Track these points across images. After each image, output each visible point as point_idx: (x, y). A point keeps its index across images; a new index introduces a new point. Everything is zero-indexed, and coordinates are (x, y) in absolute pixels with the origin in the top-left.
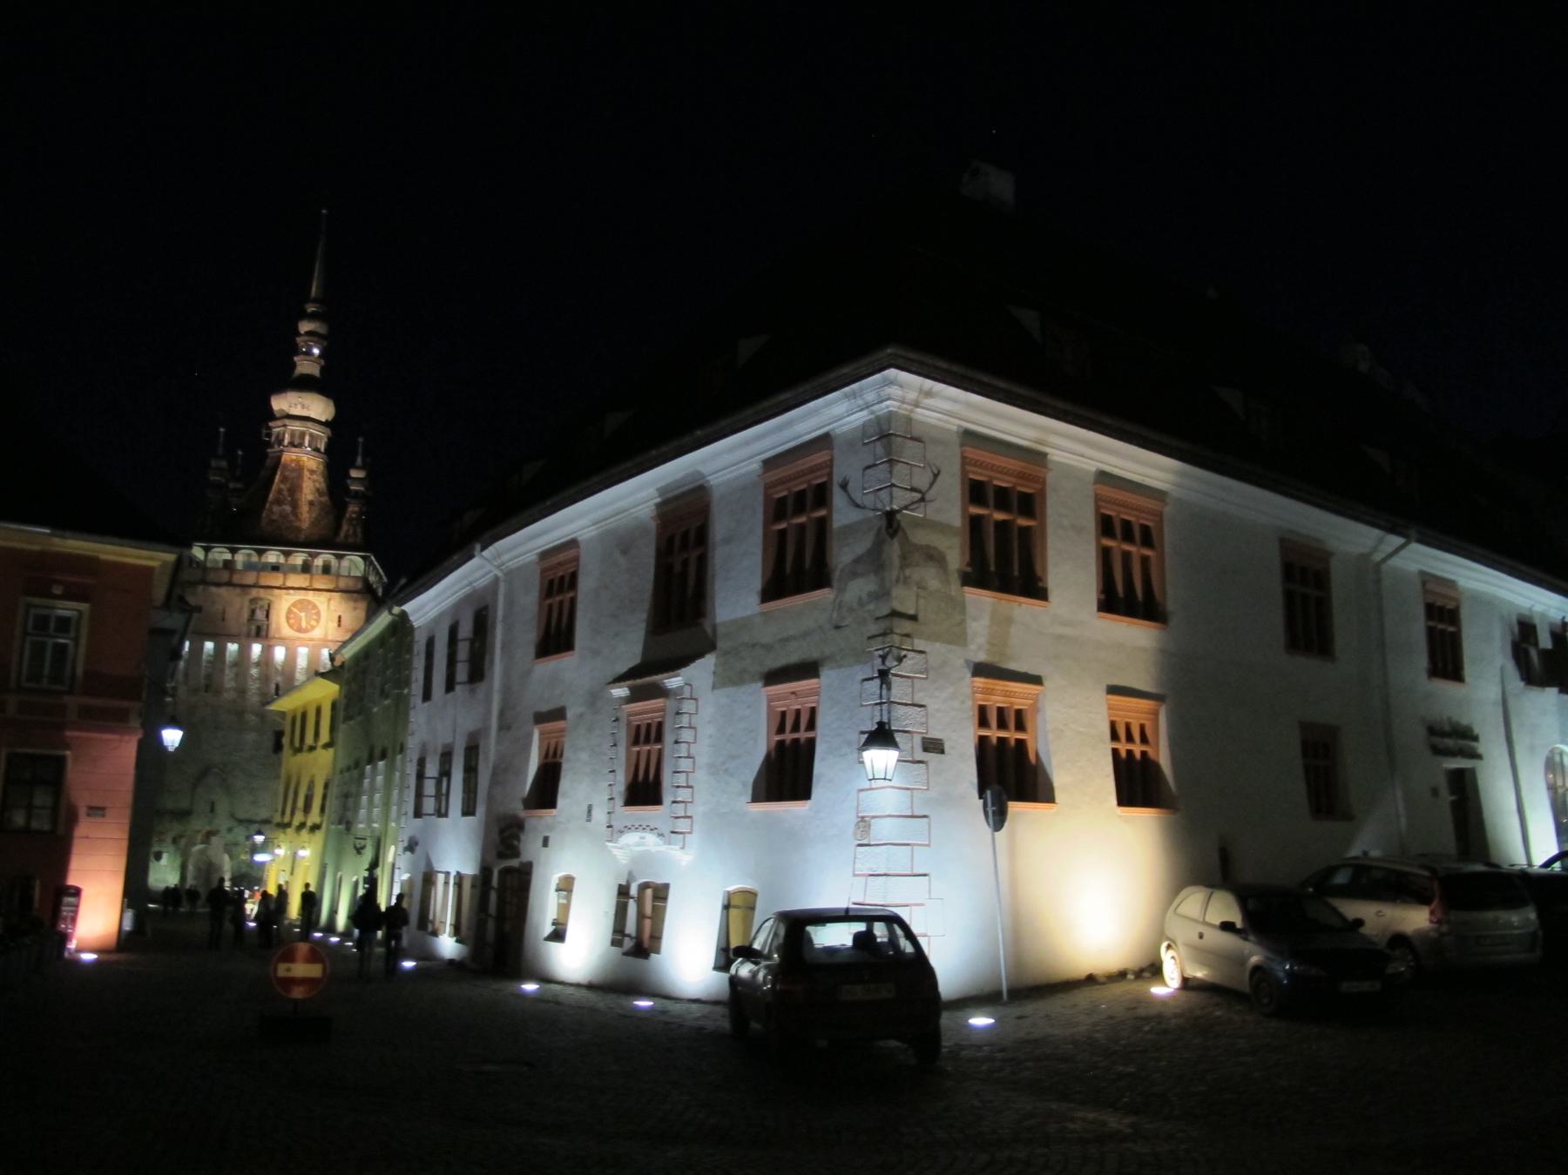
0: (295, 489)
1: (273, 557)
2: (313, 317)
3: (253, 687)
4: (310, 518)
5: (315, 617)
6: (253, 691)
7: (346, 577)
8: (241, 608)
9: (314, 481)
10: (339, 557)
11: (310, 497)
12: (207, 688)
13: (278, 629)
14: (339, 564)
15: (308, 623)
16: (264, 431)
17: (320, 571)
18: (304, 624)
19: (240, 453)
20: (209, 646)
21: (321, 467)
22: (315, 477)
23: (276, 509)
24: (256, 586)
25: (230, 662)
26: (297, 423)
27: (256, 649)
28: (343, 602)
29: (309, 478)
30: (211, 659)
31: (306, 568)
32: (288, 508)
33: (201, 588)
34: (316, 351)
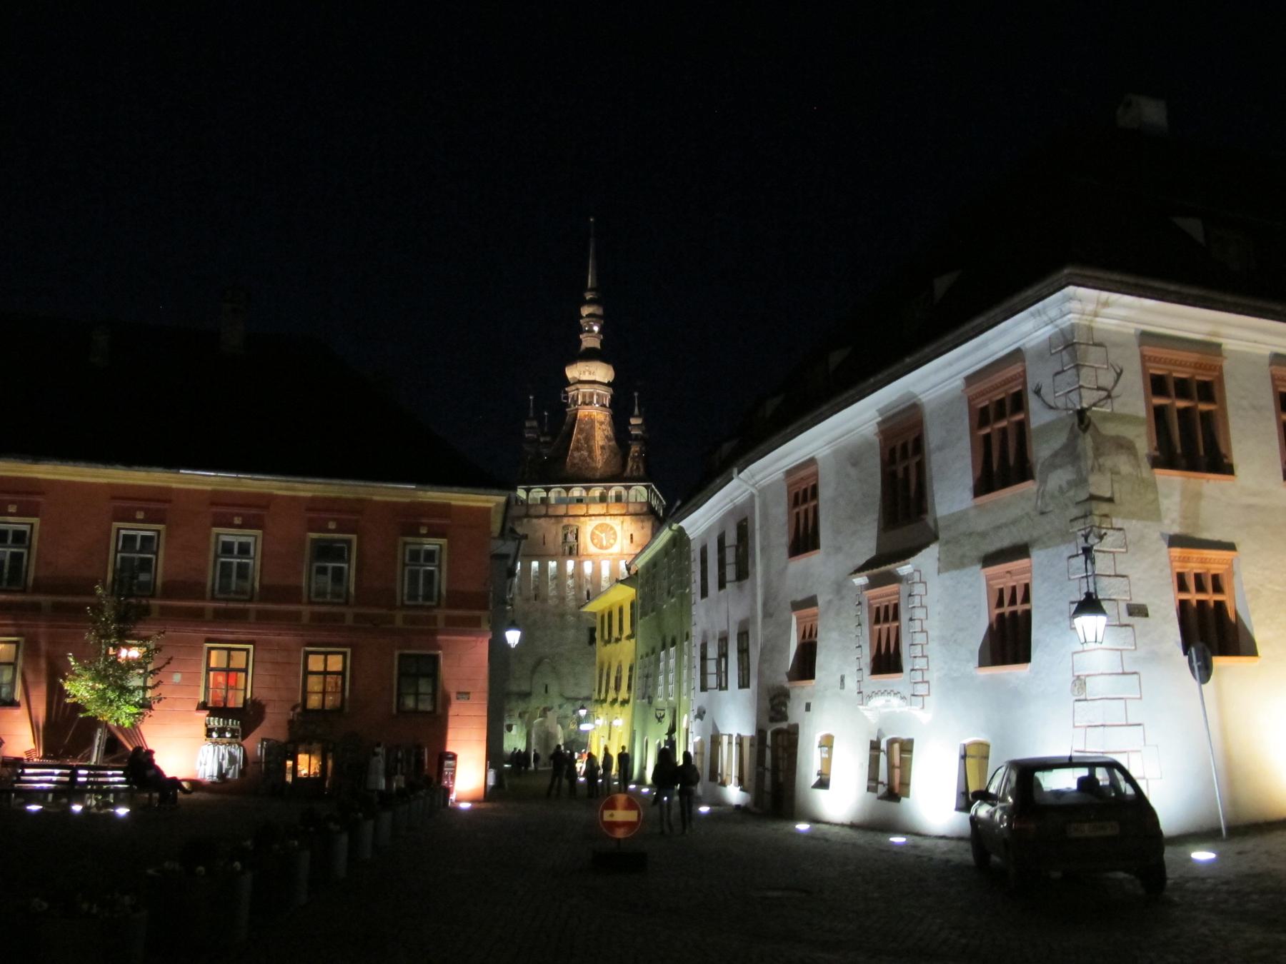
0: (589, 438)
1: (577, 492)
2: (591, 302)
3: (570, 594)
4: (603, 459)
6: (570, 598)
7: (634, 503)
8: (557, 534)
9: (603, 430)
10: (628, 488)
11: (601, 443)
12: (536, 597)
13: (586, 547)
14: (628, 493)
15: (608, 541)
16: (563, 395)
17: (614, 499)
18: (604, 543)
19: (546, 414)
20: (535, 564)
21: (608, 418)
22: (604, 427)
23: (576, 454)
24: (566, 515)
25: (551, 576)
26: (587, 386)
27: (570, 565)
30: (537, 574)
31: (603, 499)
32: (586, 453)
33: (525, 520)
34: (596, 329)
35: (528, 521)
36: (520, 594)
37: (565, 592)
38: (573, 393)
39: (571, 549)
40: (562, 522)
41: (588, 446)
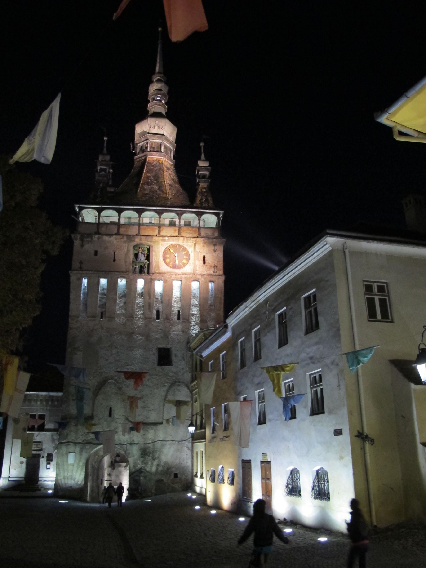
0: (158, 176)
3: (139, 313)
5: (185, 257)
8: (128, 251)
13: (158, 266)
15: (180, 261)
18: (177, 262)
20: (103, 282)
21: (172, 167)
23: (146, 187)
27: (140, 283)
28: (205, 246)
29: (167, 171)
30: (106, 292)
31: (172, 224)
32: (156, 187)
35: (99, 238)
37: (133, 309)
38: (141, 144)
39: (141, 268)
40: (134, 241)
41: (158, 182)
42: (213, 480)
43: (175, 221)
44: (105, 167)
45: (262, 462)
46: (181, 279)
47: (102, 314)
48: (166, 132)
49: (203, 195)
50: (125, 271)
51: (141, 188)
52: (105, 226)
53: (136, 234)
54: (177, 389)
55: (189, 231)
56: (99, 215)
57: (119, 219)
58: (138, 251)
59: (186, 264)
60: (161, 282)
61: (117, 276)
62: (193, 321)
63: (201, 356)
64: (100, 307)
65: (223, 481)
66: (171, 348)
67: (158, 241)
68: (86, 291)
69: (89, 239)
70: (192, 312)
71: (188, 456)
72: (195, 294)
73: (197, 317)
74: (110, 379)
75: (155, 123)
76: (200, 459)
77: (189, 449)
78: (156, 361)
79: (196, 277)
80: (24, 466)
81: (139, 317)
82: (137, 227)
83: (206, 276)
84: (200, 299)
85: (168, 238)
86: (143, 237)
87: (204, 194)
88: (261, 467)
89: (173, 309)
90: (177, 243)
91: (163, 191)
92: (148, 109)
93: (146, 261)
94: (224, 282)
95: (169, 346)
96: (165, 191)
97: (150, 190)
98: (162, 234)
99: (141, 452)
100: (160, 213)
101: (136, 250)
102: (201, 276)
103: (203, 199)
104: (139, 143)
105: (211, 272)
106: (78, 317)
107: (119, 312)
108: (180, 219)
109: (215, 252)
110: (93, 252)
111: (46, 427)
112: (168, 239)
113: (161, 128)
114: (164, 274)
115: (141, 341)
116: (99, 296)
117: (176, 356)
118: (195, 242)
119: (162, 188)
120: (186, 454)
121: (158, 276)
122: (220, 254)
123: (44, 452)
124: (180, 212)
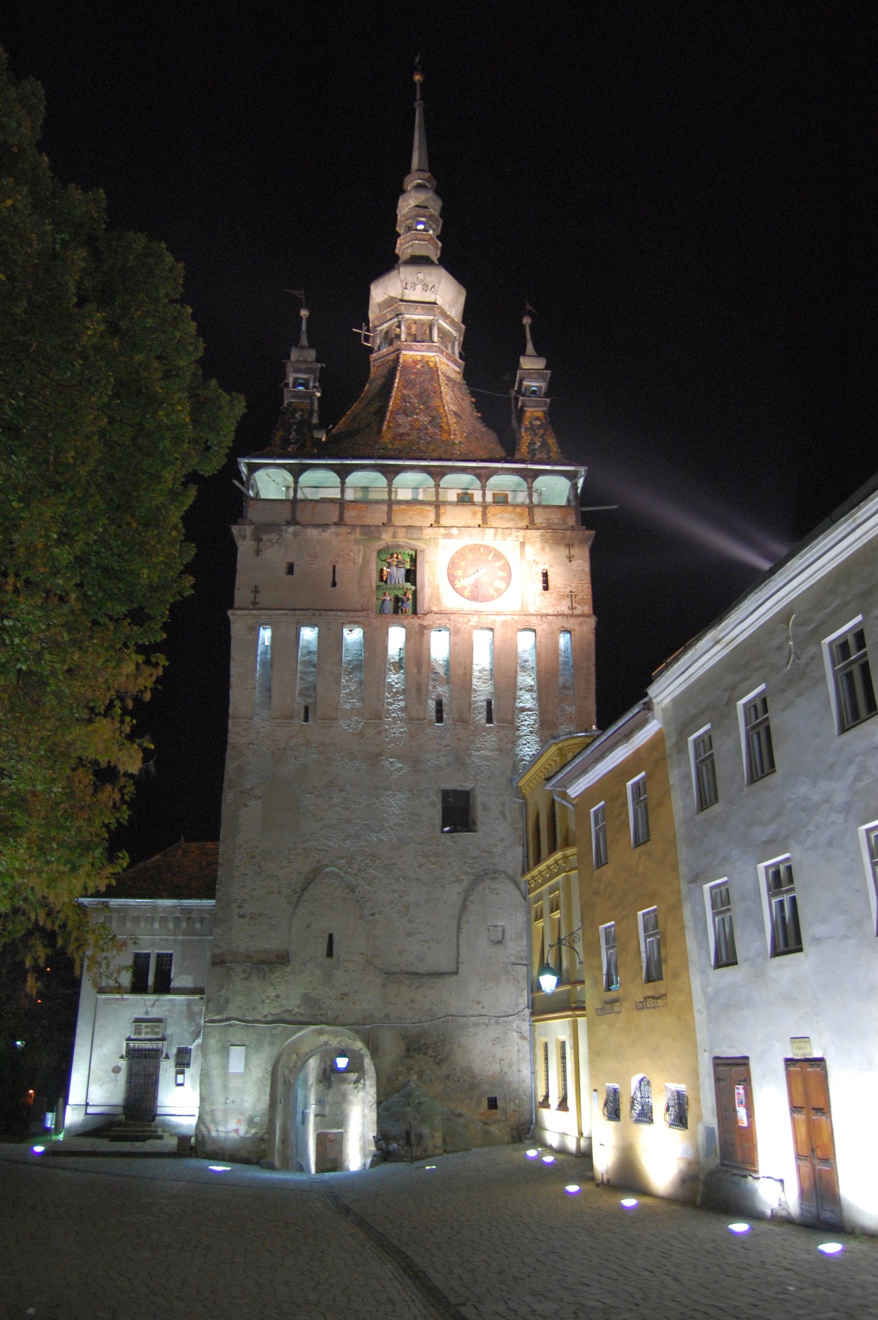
5: (501, 574)
8: (366, 563)
20: (309, 635)
23: (401, 419)
25: (349, 663)
28: (547, 549)
29: (446, 384)
30: (315, 658)
31: (465, 499)
35: (295, 535)
36: (268, 701)
37: (380, 699)
38: (385, 326)
39: (397, 599)
41: (428, 408)
42: (613, 1112)
43: (473, 494)
44: (305, 376)
45: (789, 1062)
46: (492, 627)
47: (306, 709)
48: (442, 298)
49: (536, 434)
50: (359, 607)
51: (389, 422)
52: (310, 506)
53: (383, 524)
54: (490, 888)
55: (507, 515)
56: (296, 482)
57: (343, 492)
58: (388, 562)
59: (501, 590)
60: (445, 634)
61: (341, 621)
62: (524, 725)
63: (565, 796)
64: (301, 695)
65: (645, 1116)
66: (473, 789)
67: (435, 539)
68: (269, 656)
69: (274, 537)
70: (521, 705)
71: (521, 1054)
72: (526, 661)
73: (532, 715)
74: (327, 866)
75: (415, 278)
76: (557, 1061)
77: (523, 1038)
78: (438, 820)
79: (528, 622)
80: (122, 1077)
81: (393, 718)
82: (385, 508)
83: (550, 618)
84: (538, 672)
85: (459, 531)
86: (399, 530)
87: (537, 431)
88: (789, 1075)
89: (475, 697)
90: (481, 543)
91: (441, 427)
92: (397, 251)
93: (408, 585)
94: (594, 631)
95: (467, 786)
96: (446, 427)
97: (410, 425)
98: (444, 521)
99: (406, 1044)
100: (437, 474)
101: (385, 560)
102: (539, 617)
103: (535, 443)
104: (380, 325)
105: (564, 607)
106: (252, 719)
107: (348, 706)
108: (483, 488)
109: (570, 561)
110: (284, 567)
111: (174, 984)
112: (459, 534)
113: (431, 289)
114: (453, 613)
115: (401, 773)
116: (300, 668)
117: (485, 808)
118: (522, 540)
119: (439, 421)
120: (517, 1048)
121: (439, 619)
122: (582, 563)
123: (170, 1045)
124: (483, 472)
